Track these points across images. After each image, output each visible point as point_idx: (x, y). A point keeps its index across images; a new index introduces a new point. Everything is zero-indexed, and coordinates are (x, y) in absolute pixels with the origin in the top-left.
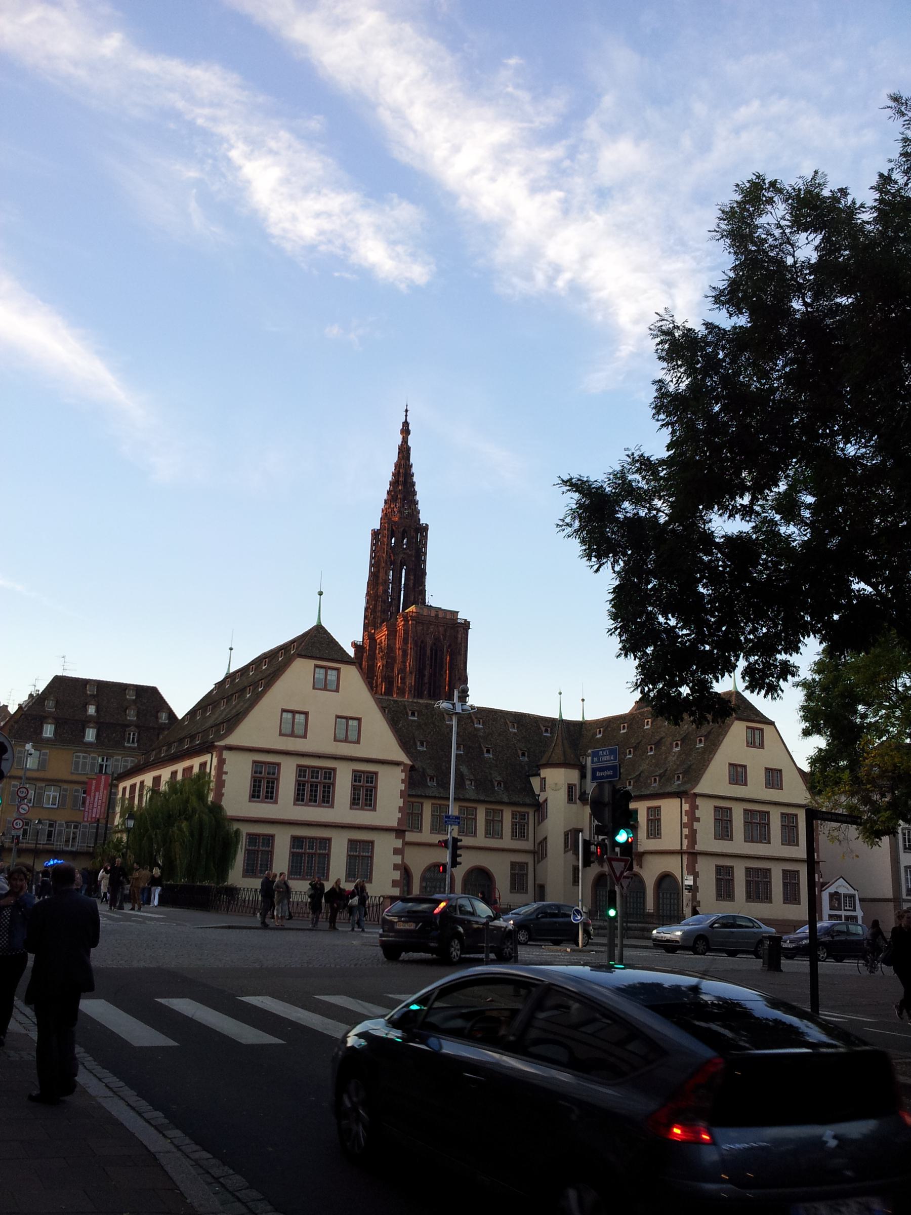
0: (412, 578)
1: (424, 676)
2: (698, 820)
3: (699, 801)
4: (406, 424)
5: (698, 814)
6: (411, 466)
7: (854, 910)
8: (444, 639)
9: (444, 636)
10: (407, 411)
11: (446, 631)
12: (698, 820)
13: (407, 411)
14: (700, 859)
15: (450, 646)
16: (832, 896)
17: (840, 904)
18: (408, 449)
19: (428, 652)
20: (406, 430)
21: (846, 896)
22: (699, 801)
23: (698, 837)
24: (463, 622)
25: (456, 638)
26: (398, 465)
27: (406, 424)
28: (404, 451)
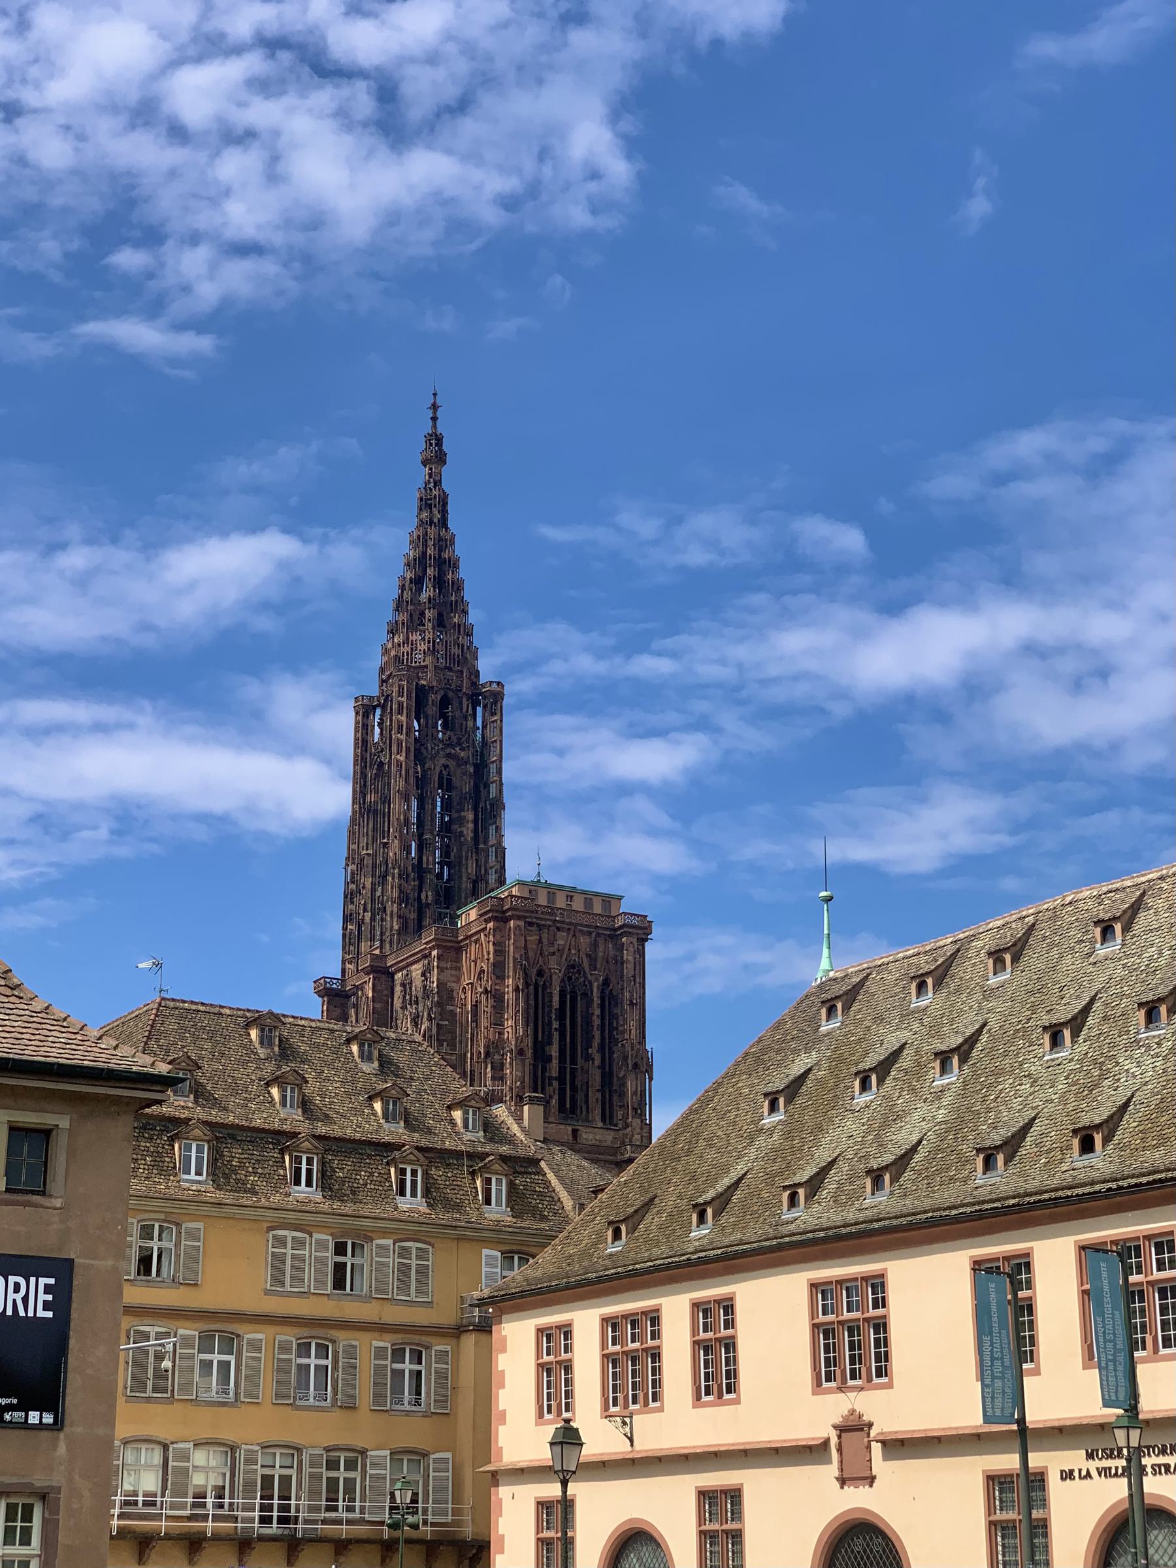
1: (549, 1059)
4: (436, 440)
6: (452, 543)
8: (593, 967)
10: (435, 407)
11: (595, 945)
13: (435, 407)
15: (606, 982)
20: (435, 453)
26: (420, 541)
27: (436, 440)
28: (434, 506)
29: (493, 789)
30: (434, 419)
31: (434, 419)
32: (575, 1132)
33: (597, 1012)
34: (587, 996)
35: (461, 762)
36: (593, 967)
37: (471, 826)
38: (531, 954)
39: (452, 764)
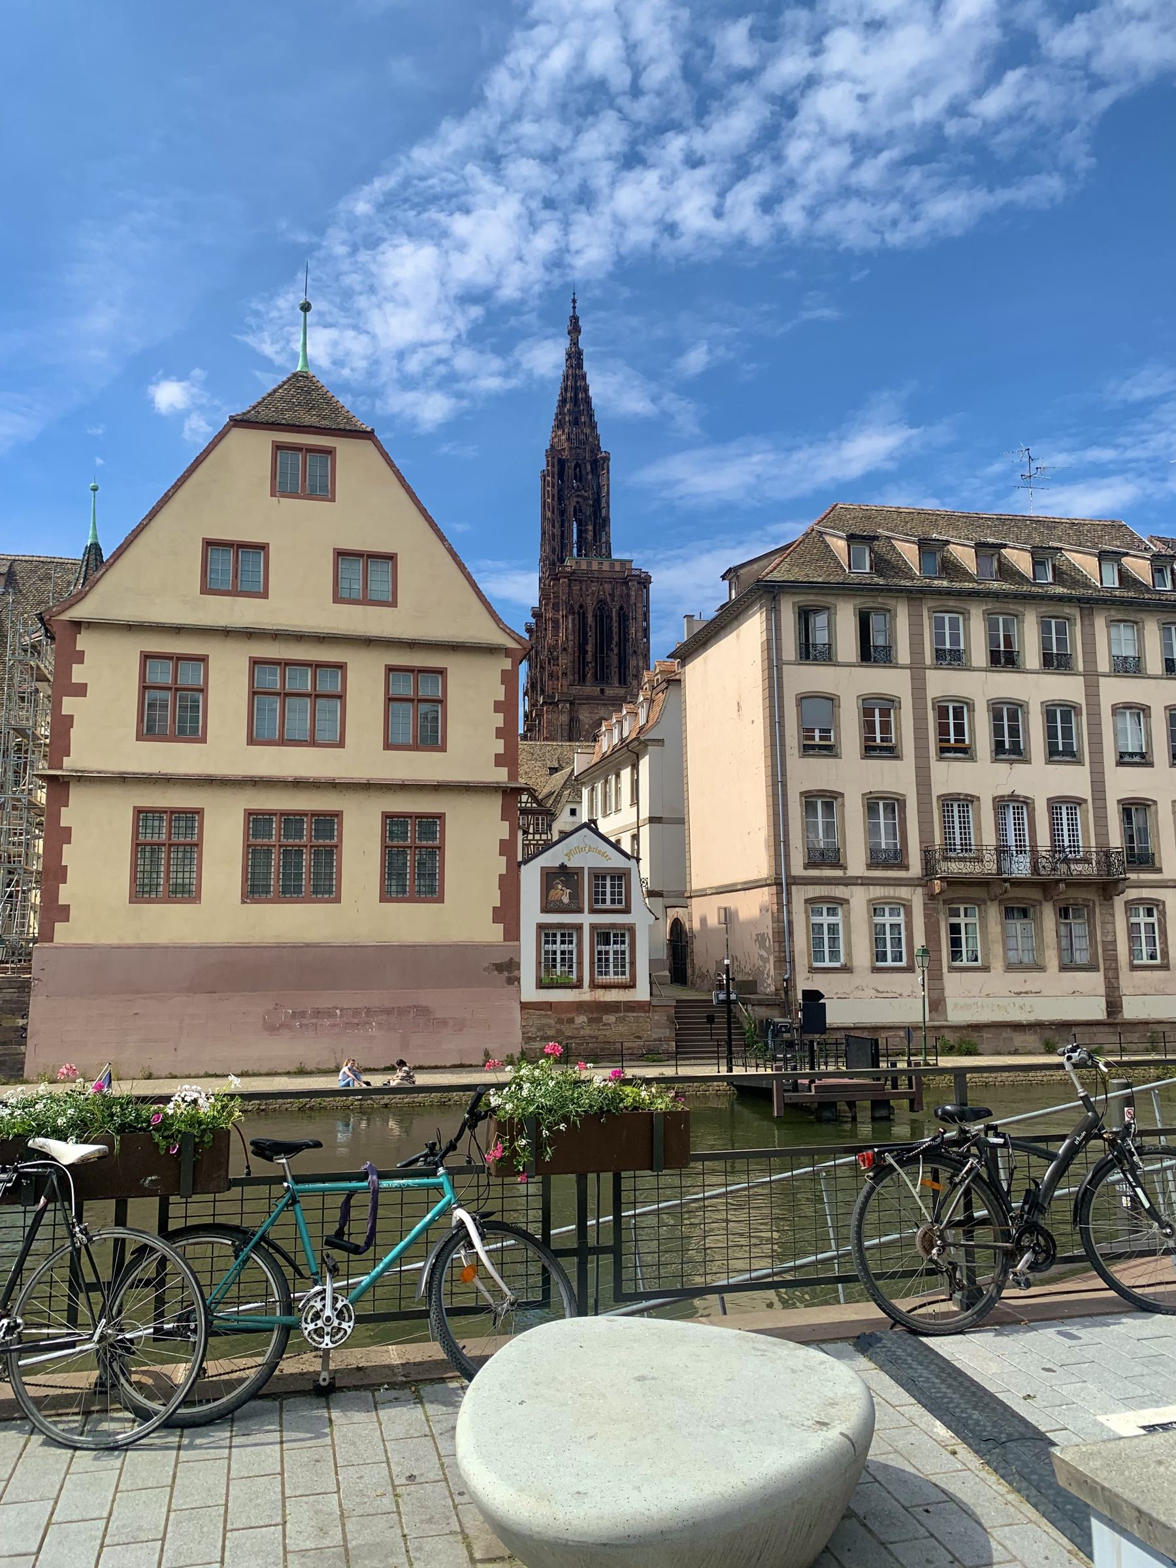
0: (590, 528)
2: (81, 690)
3: (84, 642)
5: (78, 674)
7: (627, 911)
8: (613, 600)
9: (612, 595)
10: (574, 301)
11: (613, 589)
12: (81, 690)
13: (574, 301)
14: (76, 794)
15: (621, 608)
16: (550, 877)
17: (576, 896)
18: (579, 353)
19: (590, 619)
21: (599, 876)
22: (84, 642)
23: (76, 735)
24: (638, 573)
25: (628, 596)
29: (604, 511)
30: (574, 308)
31: (574, 308)
32: (602, 691)
33: (615, 624)
34: (610, 617)
35: (586, 499)
36: (613, 600)
37: (591, 533)
38: (575, 597)
39: (580, 500)
